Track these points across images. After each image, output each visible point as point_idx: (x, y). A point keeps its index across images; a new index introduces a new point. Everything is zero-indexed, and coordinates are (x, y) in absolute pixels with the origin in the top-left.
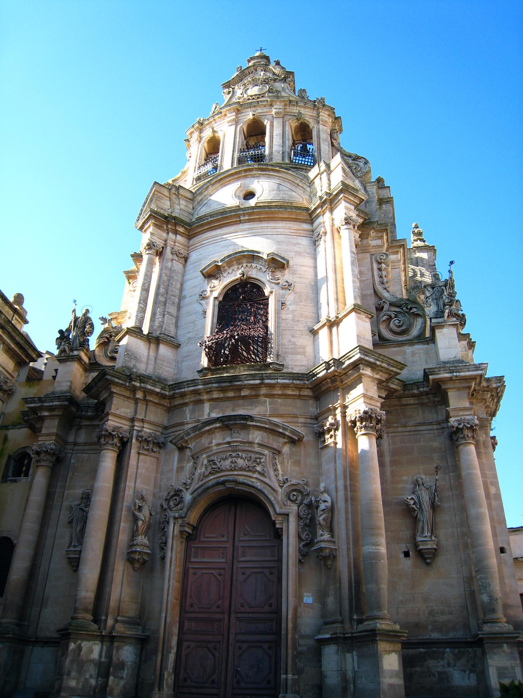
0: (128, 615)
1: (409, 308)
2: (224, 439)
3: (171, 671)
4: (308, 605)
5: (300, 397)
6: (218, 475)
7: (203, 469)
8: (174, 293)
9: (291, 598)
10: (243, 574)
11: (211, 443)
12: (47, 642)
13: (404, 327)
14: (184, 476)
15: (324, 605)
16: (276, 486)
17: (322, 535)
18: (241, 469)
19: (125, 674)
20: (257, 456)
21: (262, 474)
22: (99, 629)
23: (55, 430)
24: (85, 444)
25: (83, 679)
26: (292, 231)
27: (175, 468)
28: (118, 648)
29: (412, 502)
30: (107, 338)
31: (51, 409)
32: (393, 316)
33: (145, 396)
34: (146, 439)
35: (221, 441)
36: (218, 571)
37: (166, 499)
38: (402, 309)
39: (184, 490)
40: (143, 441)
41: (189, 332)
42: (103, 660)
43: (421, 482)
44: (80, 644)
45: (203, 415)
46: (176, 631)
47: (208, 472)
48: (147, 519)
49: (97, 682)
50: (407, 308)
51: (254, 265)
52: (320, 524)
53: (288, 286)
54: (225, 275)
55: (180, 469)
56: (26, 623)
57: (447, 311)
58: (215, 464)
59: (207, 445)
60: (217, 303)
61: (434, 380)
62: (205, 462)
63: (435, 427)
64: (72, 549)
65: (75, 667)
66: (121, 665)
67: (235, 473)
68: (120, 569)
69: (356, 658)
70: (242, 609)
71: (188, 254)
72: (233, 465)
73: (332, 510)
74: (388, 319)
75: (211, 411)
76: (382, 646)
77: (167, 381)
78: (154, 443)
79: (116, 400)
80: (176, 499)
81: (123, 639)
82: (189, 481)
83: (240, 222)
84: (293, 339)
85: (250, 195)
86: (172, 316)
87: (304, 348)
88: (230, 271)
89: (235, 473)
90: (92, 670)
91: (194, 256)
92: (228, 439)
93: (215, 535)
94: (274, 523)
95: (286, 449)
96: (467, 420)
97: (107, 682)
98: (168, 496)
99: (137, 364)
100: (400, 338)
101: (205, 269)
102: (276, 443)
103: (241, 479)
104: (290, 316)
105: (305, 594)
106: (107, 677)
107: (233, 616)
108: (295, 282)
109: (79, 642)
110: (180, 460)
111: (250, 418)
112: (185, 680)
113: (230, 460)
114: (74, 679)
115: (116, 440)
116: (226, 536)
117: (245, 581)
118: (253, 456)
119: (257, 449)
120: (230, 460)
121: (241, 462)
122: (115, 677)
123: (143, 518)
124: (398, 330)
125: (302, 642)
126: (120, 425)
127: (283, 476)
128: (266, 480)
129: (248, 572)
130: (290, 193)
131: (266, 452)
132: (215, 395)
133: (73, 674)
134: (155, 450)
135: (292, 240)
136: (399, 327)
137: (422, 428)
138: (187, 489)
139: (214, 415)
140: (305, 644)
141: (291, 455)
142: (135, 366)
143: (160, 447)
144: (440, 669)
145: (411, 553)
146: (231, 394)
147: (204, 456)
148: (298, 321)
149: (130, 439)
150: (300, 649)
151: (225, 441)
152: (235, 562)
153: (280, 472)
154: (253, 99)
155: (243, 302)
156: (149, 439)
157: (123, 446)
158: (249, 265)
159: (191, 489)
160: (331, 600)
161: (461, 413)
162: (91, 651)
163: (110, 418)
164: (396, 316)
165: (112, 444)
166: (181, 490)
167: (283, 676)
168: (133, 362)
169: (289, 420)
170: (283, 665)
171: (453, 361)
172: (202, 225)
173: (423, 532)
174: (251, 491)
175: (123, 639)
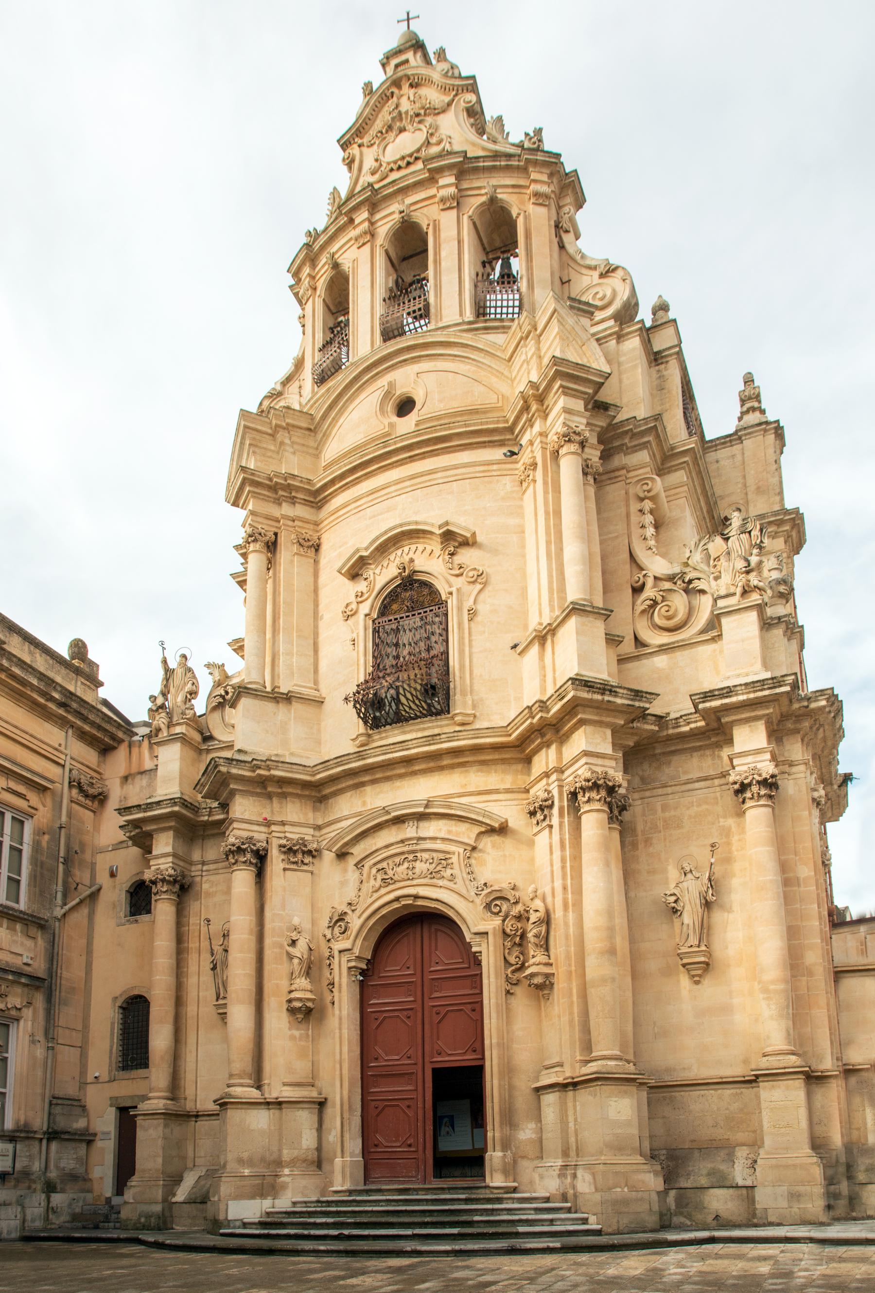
14: (350, 893)
20: (441, 856)
34: (290, 849)
39: (349, 912)
40: (289, 851)
47: (377, 885)
48: (305, 957)
53: (480, 578)
62: (374, 871)
68: (277, 1021)
72: (410, 873)
78: (304, 853)
80: (340, 926)
88: (385, 564)
89: (415, 882)
93: (398, 968)
98: (330, 922)
103: (423, 891)
113: (406, 865)
116: (412, 968)
126: (251, 834)
129: (443, 1011)
134: (306, 861)
138: (353, 911)
143: (314, 857)
152: (426, 999)
156: (295, 848)
159: (357, 913)
165: (245, 862)
166: (345, 913)
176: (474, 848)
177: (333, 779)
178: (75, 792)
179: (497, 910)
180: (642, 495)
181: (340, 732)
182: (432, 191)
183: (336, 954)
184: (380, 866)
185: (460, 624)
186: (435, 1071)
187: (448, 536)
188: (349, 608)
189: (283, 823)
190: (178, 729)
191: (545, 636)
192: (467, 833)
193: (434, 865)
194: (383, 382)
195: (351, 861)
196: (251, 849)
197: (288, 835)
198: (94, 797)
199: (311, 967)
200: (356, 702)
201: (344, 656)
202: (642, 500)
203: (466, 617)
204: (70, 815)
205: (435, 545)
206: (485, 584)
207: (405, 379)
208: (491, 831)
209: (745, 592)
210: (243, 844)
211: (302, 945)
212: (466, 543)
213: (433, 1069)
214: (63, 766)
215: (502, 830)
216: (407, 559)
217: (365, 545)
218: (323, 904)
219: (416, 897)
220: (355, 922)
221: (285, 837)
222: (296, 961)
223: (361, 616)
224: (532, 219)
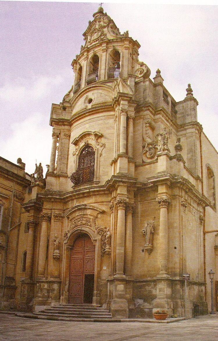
4: (105, 270)
5: (105, 194)
18: (84, 225)
19: (55, 292)
21: (90, 226)
23: (33, 214)
31: (30, 207)
33: (54, 200)
34: (56, 216)
40: (56, 217)
51: (90, 137)
65: (39, 290)
66: (54, 290)
71: (70, 134)
73: (110, 237)
75: (76, 202)
76: (116, 283)
79: (45, 203)
81: (53, 282)
83: (86, 116)
85: (90, 101)
88: (82, 141)
90: (45, 292)
91: (72, 134)
101: (73, 142)
103: (83, 229)
107: (84, 274)
111: (86, 205)
119: (89, 217)
121: (84, 222)
125: (103, 281)
129: (88, 260)
131: (92, 217)
132: (77, 197)
136: (150, 155)
143: (62, 218)
144: (149, 289)
146: (81, 196)
149: (51, 216)
154: (95, 42)
155: (87, 154)
157: (49, 219)
163: (43, 210)
164: (149, 150)
165: (45, 220)
172: (73, 120)
175: (53, 282)
176: (97, 217)
178: (15, 198)
179: (100, 234)
181: (69, 186)
182: (101, 48)
185: (97, 157)
187: (96, 135)
190: (37, 183)
191: (115, 162)
192: (95, 213)
194: (85, 96)
196: (47, 216)
198: (20, 199)
199: (59, 247)
200: (71, 178)
201: (72, 166)
202: (147, 123)
203: (99, 156)
204: (14, 204)
205: (93, 137)
206: (104, 147)
208: (101, 213)
209: (163, 150)
210: (45, 215)
211: (57, 241)
212: (101, 136)
214: (12, 192)
215: (103, 212)
216: (87, 140)
217: (77, 136)
218: (58, 231)
219: (81, 230)
224: (124, 53)
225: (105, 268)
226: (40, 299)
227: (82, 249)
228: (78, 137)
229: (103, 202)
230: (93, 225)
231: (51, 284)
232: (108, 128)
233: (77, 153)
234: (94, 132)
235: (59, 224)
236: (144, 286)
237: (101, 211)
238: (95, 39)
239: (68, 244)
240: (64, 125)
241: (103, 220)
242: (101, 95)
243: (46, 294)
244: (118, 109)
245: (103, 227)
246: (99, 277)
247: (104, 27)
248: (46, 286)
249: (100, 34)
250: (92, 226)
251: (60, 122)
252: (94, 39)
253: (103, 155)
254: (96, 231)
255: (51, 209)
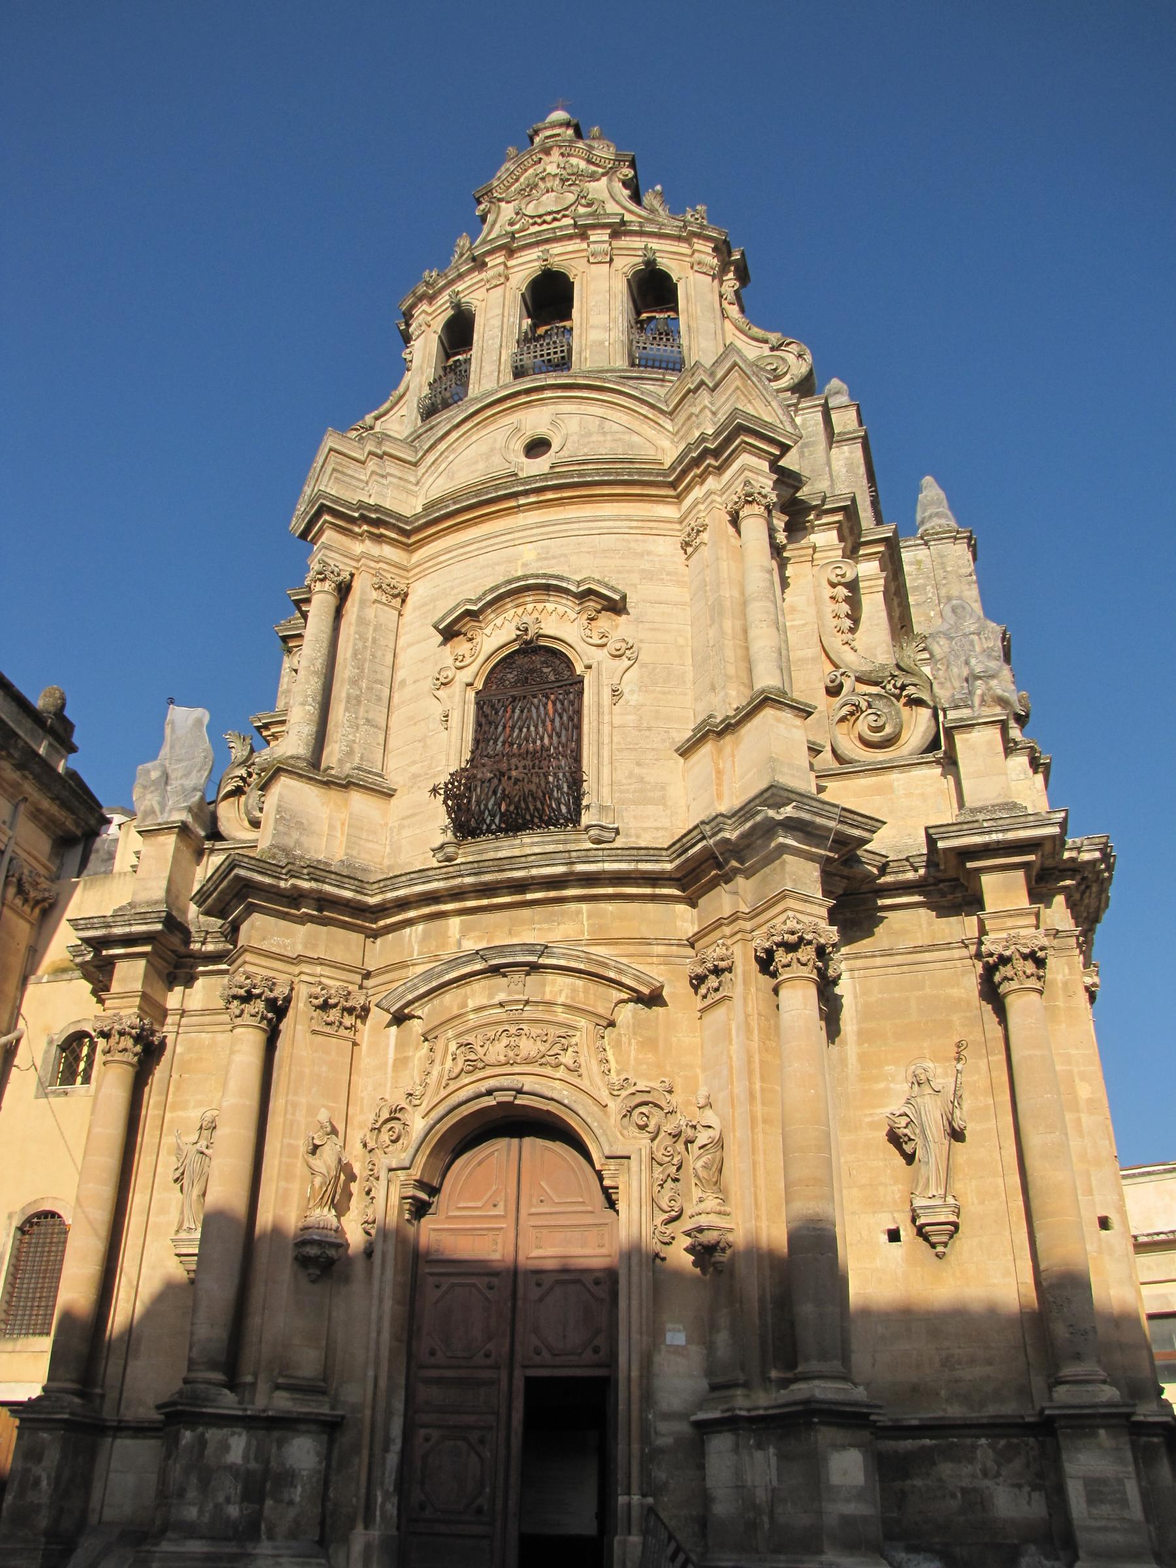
0: (300, 1373)
1: (898, 685)
2: (491, 996)
3: (391, 1489)
4: (676, 1350)
6: (481, 1074)
7: (449, 1063)
8: (378, 677)
9: (635, 1336)
10: (539, 1285)
11: (465, 1005)
12: (140, 1430)
13: (888, 730)
14: (411, 1079)
15: (710, 1347)
16: (604, 1095)
17: (701, 1200)
18: (528, 1061)
19: (297, 1494)
20: (562, 1031)
22: (240, 1403)
24: (204, 1012)
25: (211, 1505)
26: (634, 524)
27: (391, 1061)
28: (281, 1443)
29: (903, 1121)
30: (242, 778)
31: (129, 940)
32: (864, 705)
35: (485, 1002)
36: (486, 1279)
37: (373, 1129)
38: (884, 688)
41: (414, 763)
42: (253, 1465)
43: (923, 1077)
44: (203, 1434)
45: (444, 945)
46: (399, 1405)
47: (457, 1070)
49: (241, 1510)
50: (895, 686)
51: (550, 606)
52: (697, 1176)
54: (487, 631)
55: (401, 1062)
56: (98, 1391)
57: (979, 692)
58: (472, 1050)
59: (455, 1012)
60: (471, 695)
61: (945, 850)
62: (453, 1046)
63: (957, 953)
64: (183, 1235)
65: (194, 1480)
66: (287, 1477)
67: (516, 1069)
69: (773, 1461)
70: (537, 1359)
72: (511, 1054)
74: (852, 714)
75: (465, 931)
76: (825, 1435)
77: (370, 871)
82: (418, 1091)
84: (637, 770)
86: (376, 727)
87: (663, 788)
88: (499, 622)
89: (516, 1069)
90: (228, 1487)
92: (502, 997)
93: (479, 1204)
94: (599, 1175)
95: (627, 1013)
96: (1024, 937)
97: (260, 1512)
99: (304, 839)
100: (880, 756)
101: (443, 619)
102: (603, 999)
103: (529, 1083)
104: (631, 719)
105: (669, 1326)
106: (261, 1502)
107: (518, 1374)
108: (641, 641)
109: (201, 1429)
110: (401, 1045)
112: (422, 1508)
114: (194, 1504)
115: (260, 1006)
116: (501, 1205)
117: (541, 1299)
118: (553, 1031)
119: (561, 1015)
120: (505, 1041)
121: (528, 1047)
122: (278, 1501)
123: (324, 1171)
124: (876, 737)
125: (663, 1427)
126: (271, 974)
127: (618, 1073)
128: (584, 1084)
130: (627, 437)
131: (582, 1022)
133: (192, 1494)
135: (632, 545)
137: (927, 956)
139: (470, 945)
140: (667, 1433)
141: (637, 1025)
142: (298, 843)
145: (902, 1233)
147: (450, 1034)
148: (649, 729)
150: (660, 1442)
151: (496, 1000)
153: (613, 1065)
158: (540, 606)
159: (424, 1108)
160: (722, 1338)
161: (1010, 922)
162: (225, 1448)
164: (870, 706)
167: (622, 1500)
168: (295, 835)
169: (632, 949)
170: (621, 1476)
171: (993, 806)
173: (927, 1185)
174: (549, 1108)
177: (403, 904)
180: (835, 580)
183: (383, 1175)
184: (463, 1040)
186: (531, 1383)
188: (444, 674)
189: (320, 961)
193: (548, 1045)
195: (416, 1026)
197: (323, 980)
207: (534, 420)
213: (528, 1380)
220: (418, 1124)
221: (320, 983)
222: (318, 1180)
223: (457, 687)
225: (676, 1337)
226: (196, 1547)
227: (499, 1211)
228: (480, 599)
229: (645, 941)
230: (590, 1065)
231: (276, 1434)
232: (648, 576)
233: (466, 675)
234: (579, 584)
235: (337, 1047)
236: (927, 1458)
237: (646, 991)
238: (549, 213)
239: (416, 1173)
240: (379, 539)
241: (650, 1044)
242: (601, 426)
243: (233, 1511)
244: (712, 494)
245: (655, 1084)
246: (648, 1397)
247: (594, 177)
248: (238, 1448)
249: (571, 198)
250: (583, 1070)
251: (364, 519)
252: (541, 211)
253: (631, 697)
254: (613, 1105)
255: (299, 960)
